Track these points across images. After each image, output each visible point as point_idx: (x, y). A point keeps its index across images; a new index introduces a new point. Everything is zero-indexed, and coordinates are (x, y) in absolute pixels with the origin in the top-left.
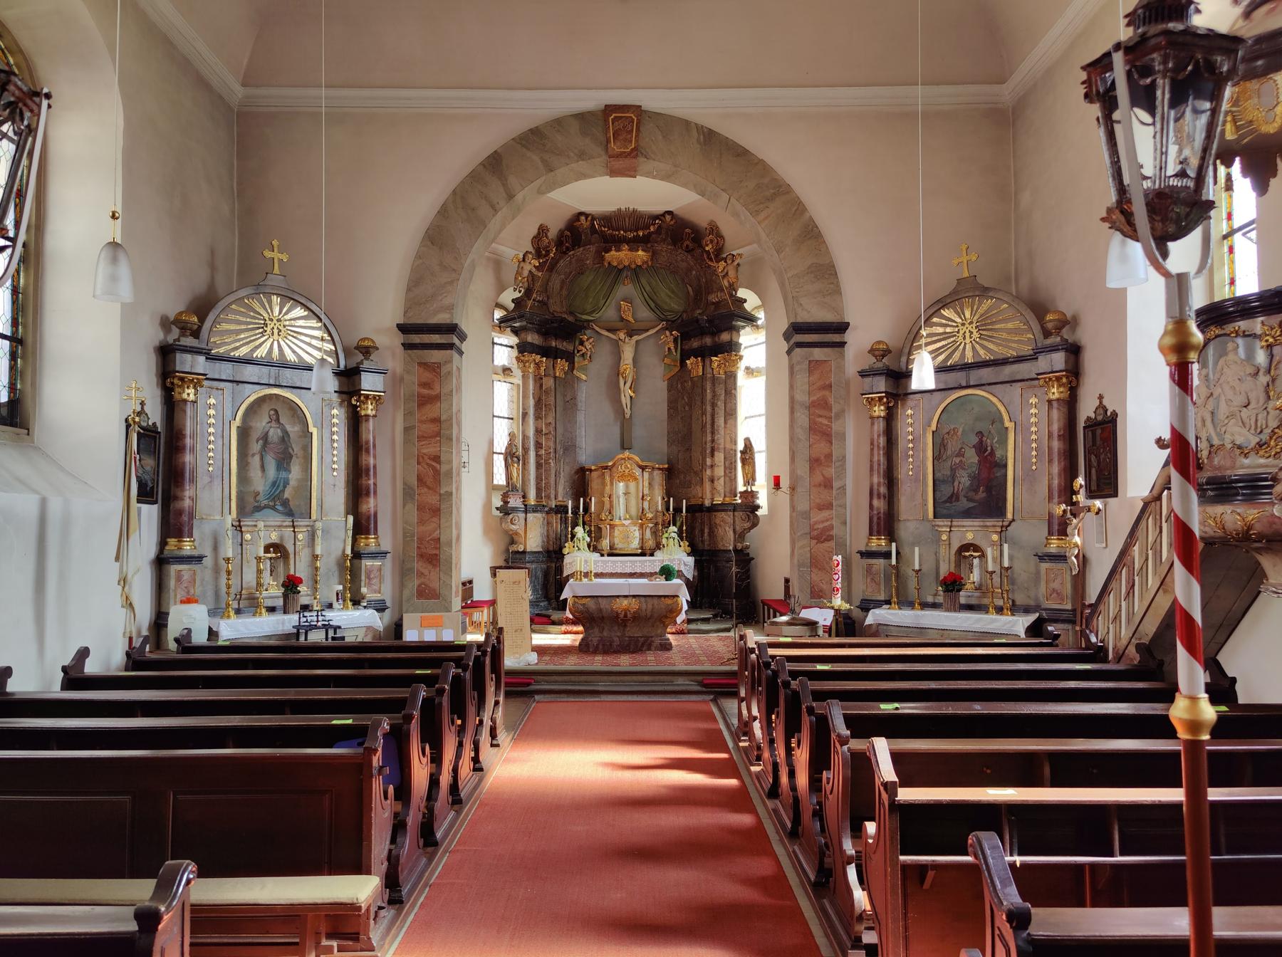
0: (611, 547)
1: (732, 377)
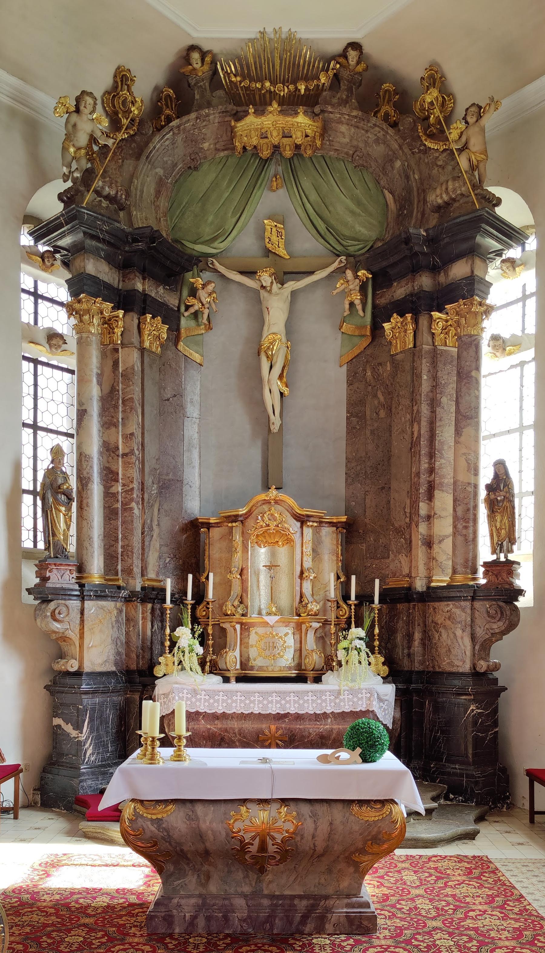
0: (244, 665)
1: (469, 347)
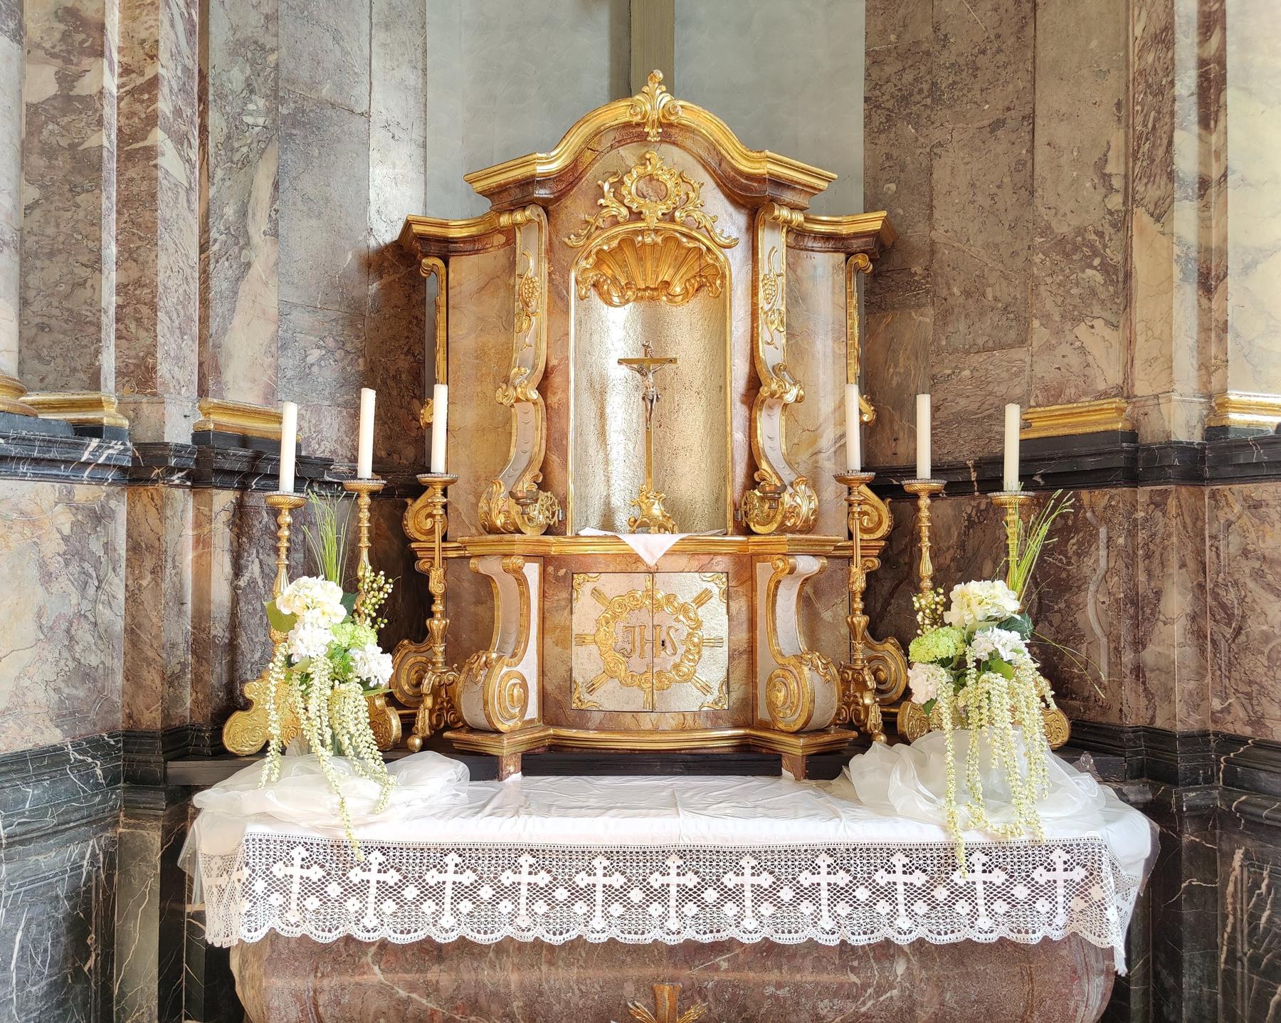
0: (554, 705)
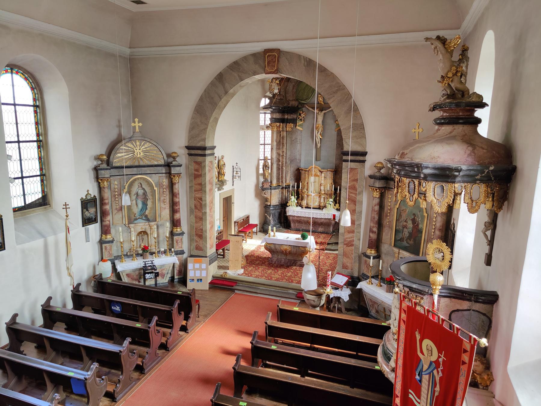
0: (307, 204)
